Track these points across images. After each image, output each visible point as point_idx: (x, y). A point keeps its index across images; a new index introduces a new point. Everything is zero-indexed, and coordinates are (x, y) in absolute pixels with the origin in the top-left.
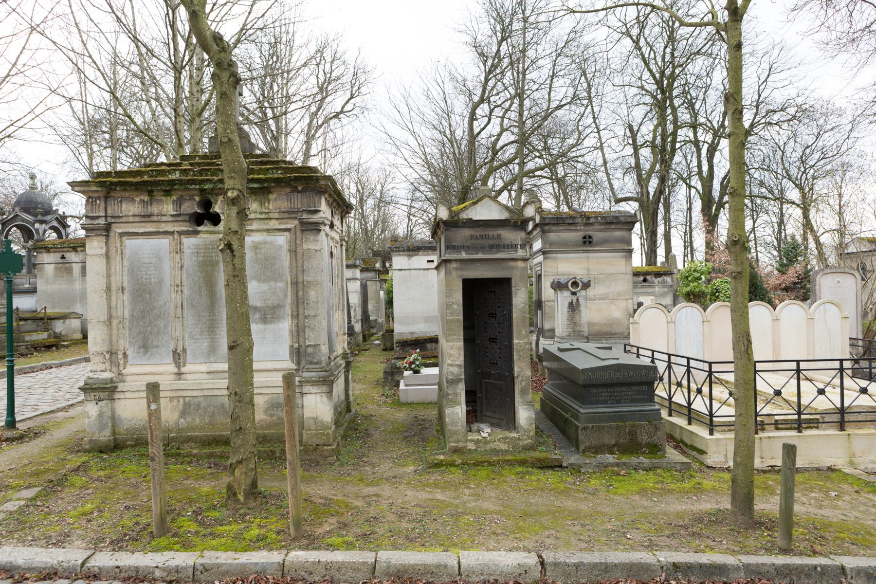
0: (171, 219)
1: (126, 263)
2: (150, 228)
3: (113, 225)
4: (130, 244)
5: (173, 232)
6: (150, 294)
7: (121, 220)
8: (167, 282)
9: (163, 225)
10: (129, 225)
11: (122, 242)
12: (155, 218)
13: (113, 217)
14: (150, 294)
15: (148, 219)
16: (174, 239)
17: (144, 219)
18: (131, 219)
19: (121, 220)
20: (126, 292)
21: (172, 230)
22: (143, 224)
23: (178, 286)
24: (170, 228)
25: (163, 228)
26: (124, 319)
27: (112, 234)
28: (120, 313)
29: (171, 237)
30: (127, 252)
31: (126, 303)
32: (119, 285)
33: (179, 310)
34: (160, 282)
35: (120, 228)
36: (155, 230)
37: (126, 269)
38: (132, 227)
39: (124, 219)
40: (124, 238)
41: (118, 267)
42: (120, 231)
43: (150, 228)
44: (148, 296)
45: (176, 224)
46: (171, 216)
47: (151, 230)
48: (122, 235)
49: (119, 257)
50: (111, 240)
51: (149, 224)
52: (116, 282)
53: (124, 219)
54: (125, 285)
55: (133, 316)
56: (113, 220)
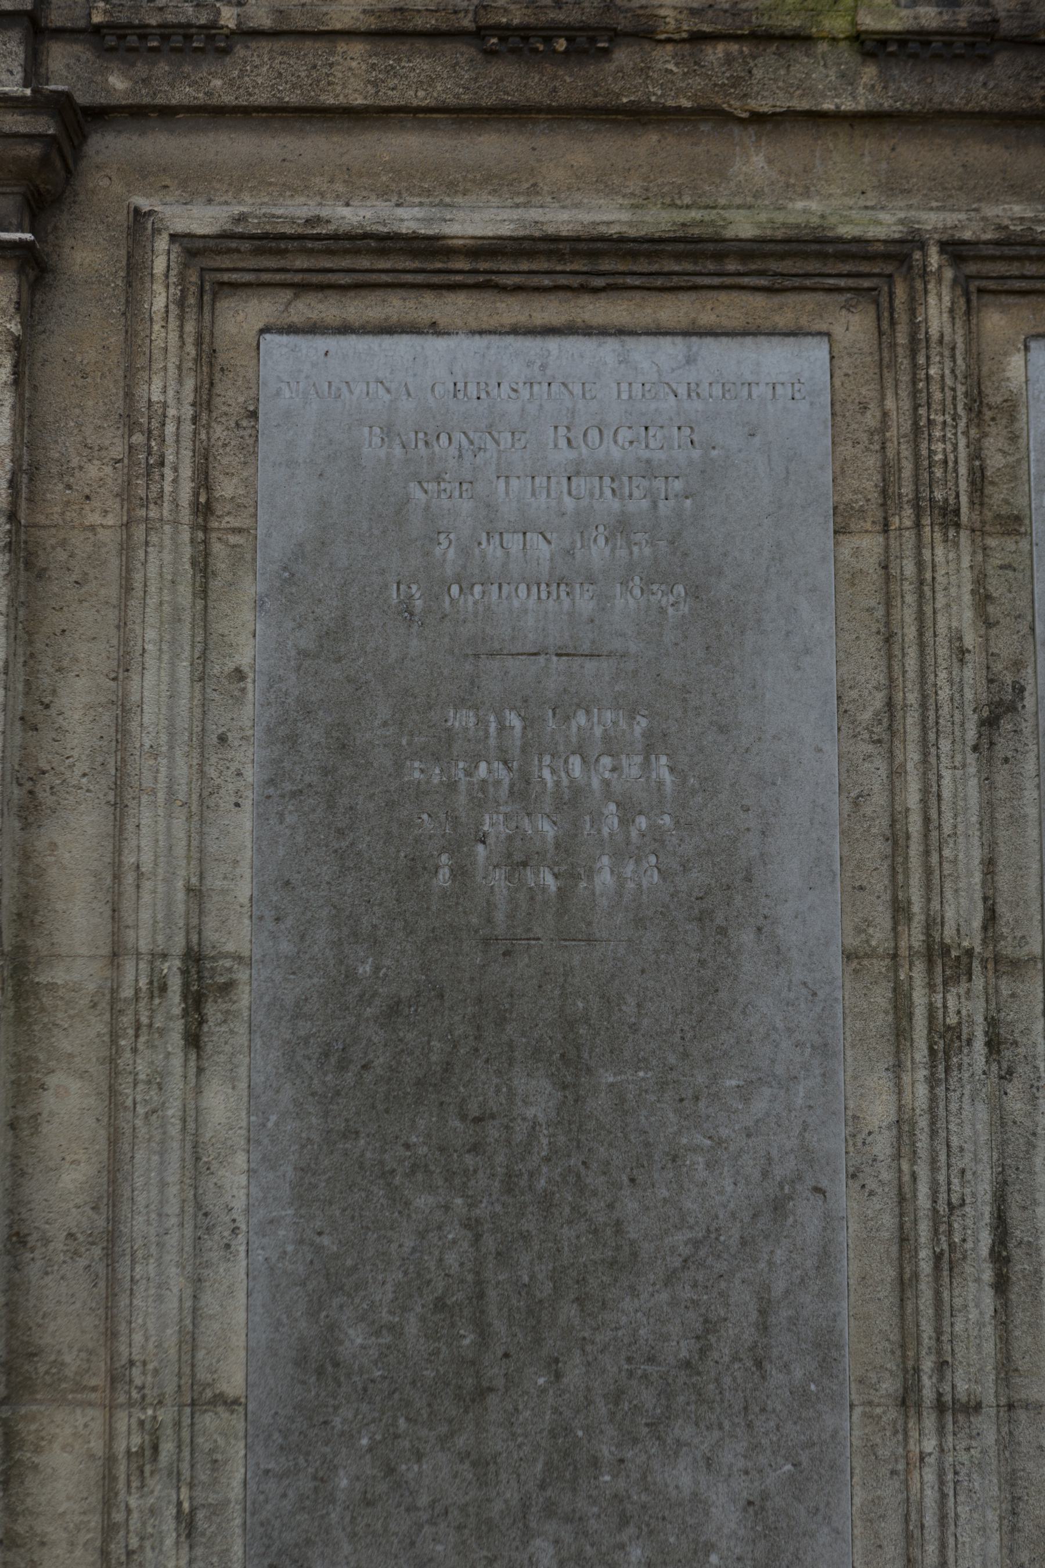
0: (864, 89)
1: (249, 638)
2: (585, 190)
3: (108, 147)
4: (327, 382)
5: (901, 254)
6: (570, 1067)
7: (214, 84)
8: (812, 905)
9: (755, 162)
10: (315, 146)
11: (207, 360)
12: (663, 76)
13: (113, 40)
14: (570, 1067)
15: (570, 84)
16: (899, 347)
17: (513, 81)
18: (351, 76)
19: (214, 84)
20: (231, 1033)
21: (885, 223)
22: (490, 146)
23: (947, 962)
24: (845, 197)
25: (758, 190)
26: (200, 1398)
27: (87, 255)
28: (151, 1326)
29: (854, 326)
30: (280, 494)
31: (234, 1183)
32: (154, 920)
33: (975, 1297)
34: (712, 910)
35: (195, 183)
36: (658, 220)
37: (250, 713)
38: (354, 182)
39: (260, 75)
40: (242, 317)
41: (159, 688)
42: (203, 219)
43: (585, 190)
44: (537, 1098)
45: (918, 155)
46: (873, 47)
47: (609, 215)
48: (218, 267)
49: (166, 557)
50: (83, 331)
51: (570, 153)
52: (116, 881)
53: (260, 75)
54: (234, 934)
55: (319, 1363)
56: (118, 84)
